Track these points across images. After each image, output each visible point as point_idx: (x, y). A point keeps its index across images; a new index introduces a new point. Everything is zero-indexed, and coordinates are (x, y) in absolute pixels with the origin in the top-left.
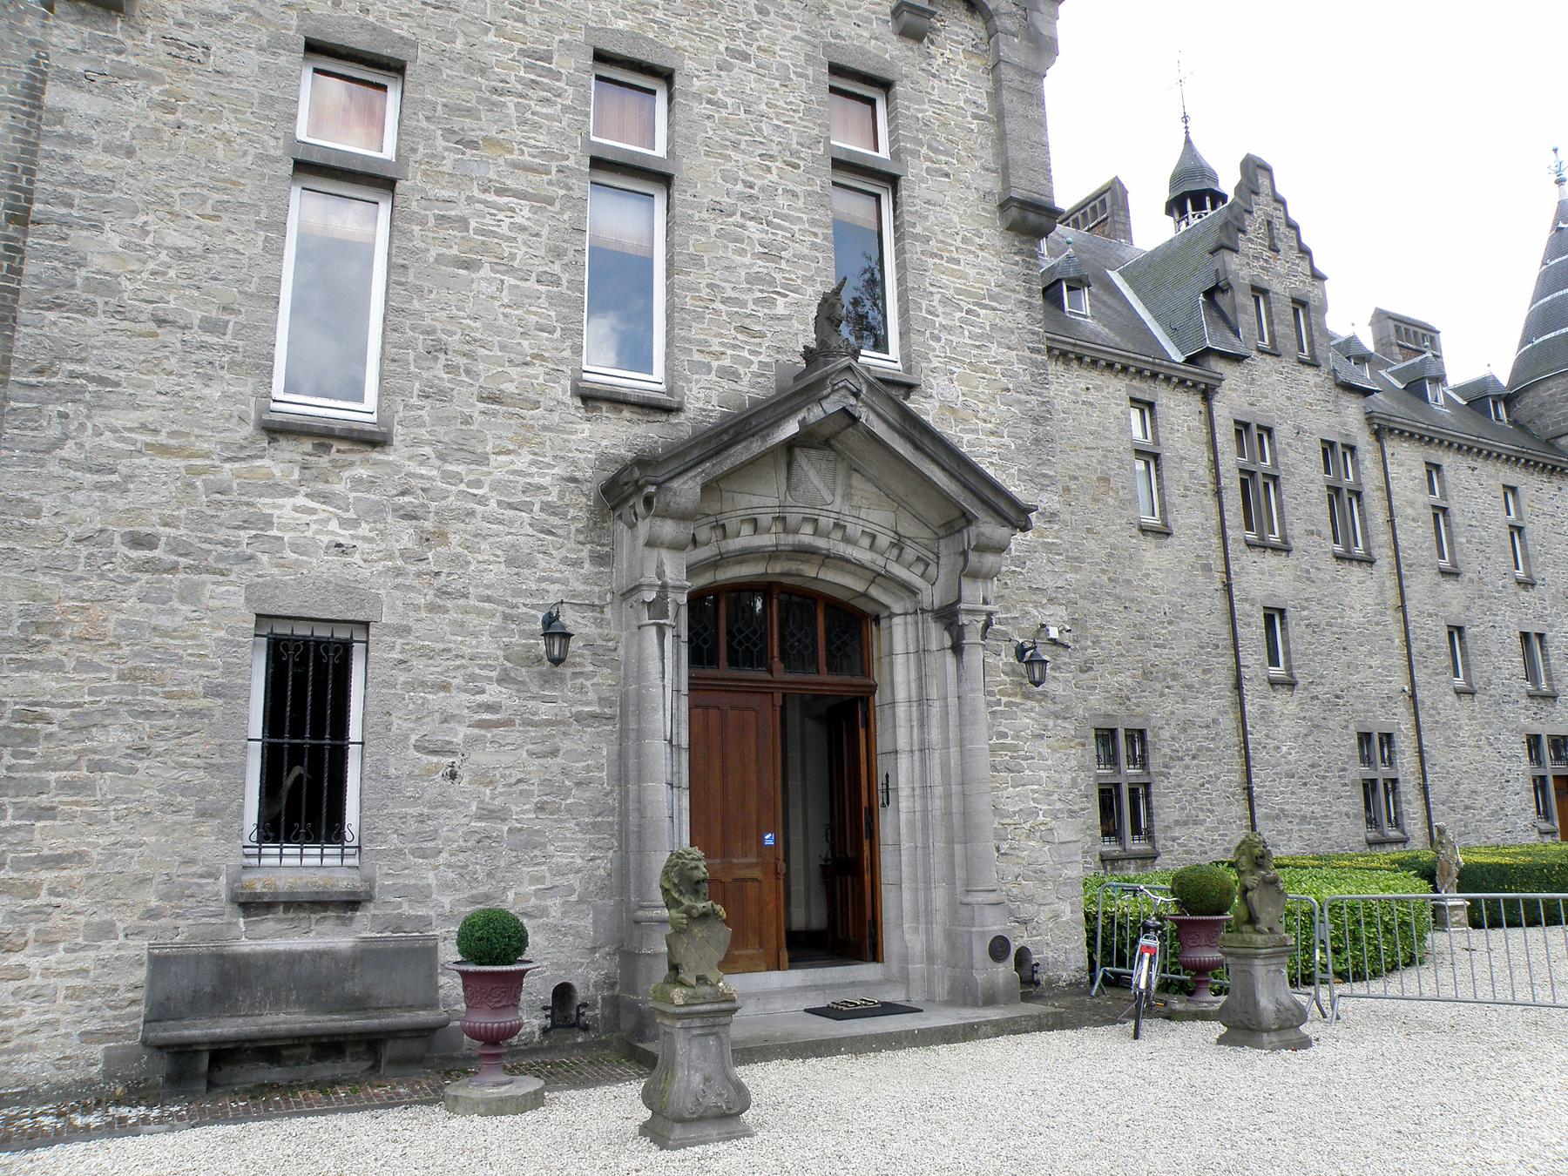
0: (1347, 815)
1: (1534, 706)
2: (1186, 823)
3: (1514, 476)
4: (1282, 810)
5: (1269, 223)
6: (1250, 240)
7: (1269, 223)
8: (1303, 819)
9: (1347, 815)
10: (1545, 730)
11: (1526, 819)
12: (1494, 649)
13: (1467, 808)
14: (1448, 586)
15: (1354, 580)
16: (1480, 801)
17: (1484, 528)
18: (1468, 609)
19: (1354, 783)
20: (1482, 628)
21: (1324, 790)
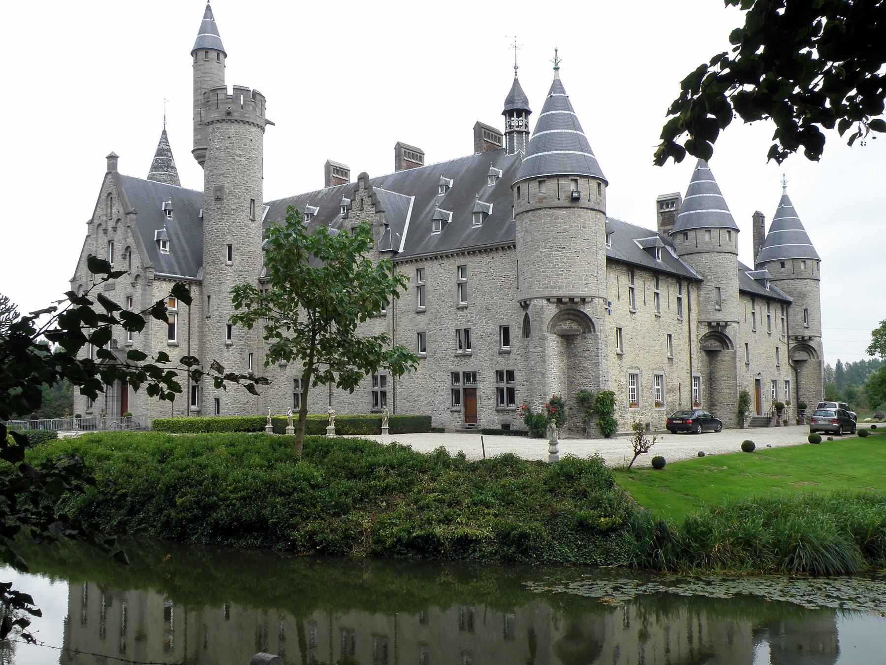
0: (365, 403)
1: (457, 360)
2: (314, 404)
3: (461, 261)
4: (343, 401)
5: (362, 199)
6: (353, 211)
7: (362, 199)
8: (349, 404)
9: (365, 403)
10: (461, 369)
11: (445, 405)
12: (439, 339)
13: (415, 401)
14: (420, 318)
15: (377, 323)
16: (423, 398)
17: (443, 289)
18: (429, 324)
19: (368, 392)
20: (435, 331)
21: (358, 394)
